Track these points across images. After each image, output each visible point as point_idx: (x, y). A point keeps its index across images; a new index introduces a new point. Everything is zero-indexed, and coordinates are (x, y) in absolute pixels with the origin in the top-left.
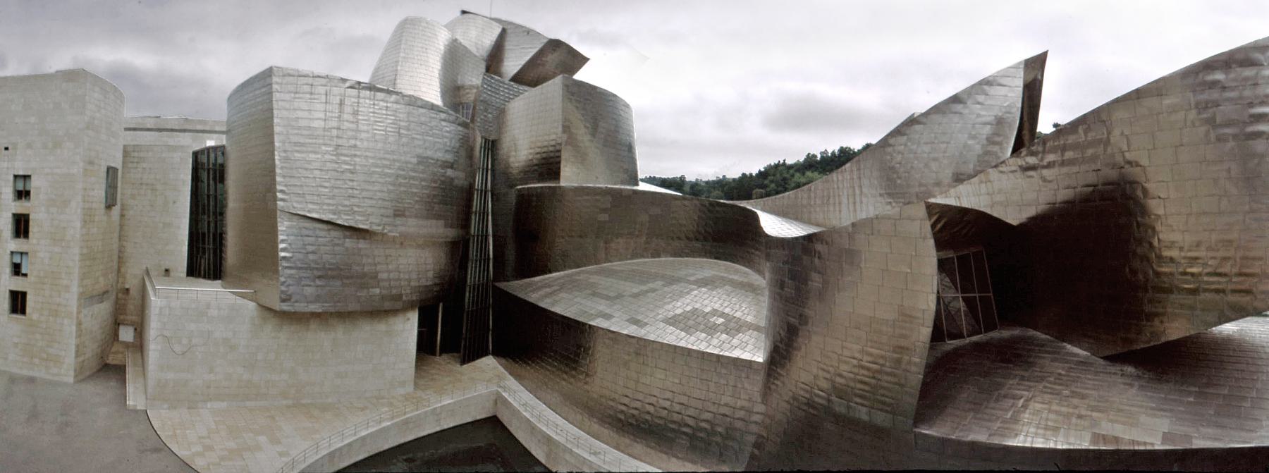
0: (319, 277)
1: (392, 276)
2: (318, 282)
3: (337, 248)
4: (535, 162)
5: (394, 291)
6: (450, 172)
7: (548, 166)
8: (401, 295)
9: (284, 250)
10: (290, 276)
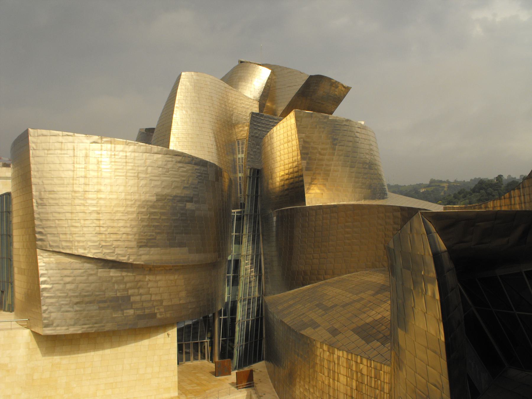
0: (77, 303)
1: (144, 298)
2: (77, 308)
3: (91, 278)
4: (286, 187)
5: (147, 311)
6: (189, 206)
7: (295, 189)
8: (155, 314)
9: (44, 282)
10: (52, 304)
